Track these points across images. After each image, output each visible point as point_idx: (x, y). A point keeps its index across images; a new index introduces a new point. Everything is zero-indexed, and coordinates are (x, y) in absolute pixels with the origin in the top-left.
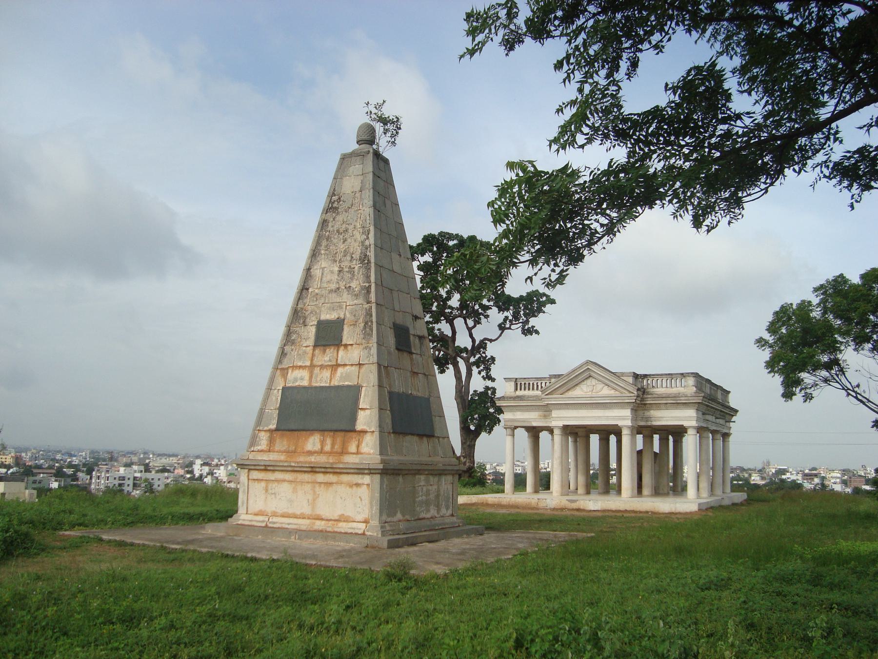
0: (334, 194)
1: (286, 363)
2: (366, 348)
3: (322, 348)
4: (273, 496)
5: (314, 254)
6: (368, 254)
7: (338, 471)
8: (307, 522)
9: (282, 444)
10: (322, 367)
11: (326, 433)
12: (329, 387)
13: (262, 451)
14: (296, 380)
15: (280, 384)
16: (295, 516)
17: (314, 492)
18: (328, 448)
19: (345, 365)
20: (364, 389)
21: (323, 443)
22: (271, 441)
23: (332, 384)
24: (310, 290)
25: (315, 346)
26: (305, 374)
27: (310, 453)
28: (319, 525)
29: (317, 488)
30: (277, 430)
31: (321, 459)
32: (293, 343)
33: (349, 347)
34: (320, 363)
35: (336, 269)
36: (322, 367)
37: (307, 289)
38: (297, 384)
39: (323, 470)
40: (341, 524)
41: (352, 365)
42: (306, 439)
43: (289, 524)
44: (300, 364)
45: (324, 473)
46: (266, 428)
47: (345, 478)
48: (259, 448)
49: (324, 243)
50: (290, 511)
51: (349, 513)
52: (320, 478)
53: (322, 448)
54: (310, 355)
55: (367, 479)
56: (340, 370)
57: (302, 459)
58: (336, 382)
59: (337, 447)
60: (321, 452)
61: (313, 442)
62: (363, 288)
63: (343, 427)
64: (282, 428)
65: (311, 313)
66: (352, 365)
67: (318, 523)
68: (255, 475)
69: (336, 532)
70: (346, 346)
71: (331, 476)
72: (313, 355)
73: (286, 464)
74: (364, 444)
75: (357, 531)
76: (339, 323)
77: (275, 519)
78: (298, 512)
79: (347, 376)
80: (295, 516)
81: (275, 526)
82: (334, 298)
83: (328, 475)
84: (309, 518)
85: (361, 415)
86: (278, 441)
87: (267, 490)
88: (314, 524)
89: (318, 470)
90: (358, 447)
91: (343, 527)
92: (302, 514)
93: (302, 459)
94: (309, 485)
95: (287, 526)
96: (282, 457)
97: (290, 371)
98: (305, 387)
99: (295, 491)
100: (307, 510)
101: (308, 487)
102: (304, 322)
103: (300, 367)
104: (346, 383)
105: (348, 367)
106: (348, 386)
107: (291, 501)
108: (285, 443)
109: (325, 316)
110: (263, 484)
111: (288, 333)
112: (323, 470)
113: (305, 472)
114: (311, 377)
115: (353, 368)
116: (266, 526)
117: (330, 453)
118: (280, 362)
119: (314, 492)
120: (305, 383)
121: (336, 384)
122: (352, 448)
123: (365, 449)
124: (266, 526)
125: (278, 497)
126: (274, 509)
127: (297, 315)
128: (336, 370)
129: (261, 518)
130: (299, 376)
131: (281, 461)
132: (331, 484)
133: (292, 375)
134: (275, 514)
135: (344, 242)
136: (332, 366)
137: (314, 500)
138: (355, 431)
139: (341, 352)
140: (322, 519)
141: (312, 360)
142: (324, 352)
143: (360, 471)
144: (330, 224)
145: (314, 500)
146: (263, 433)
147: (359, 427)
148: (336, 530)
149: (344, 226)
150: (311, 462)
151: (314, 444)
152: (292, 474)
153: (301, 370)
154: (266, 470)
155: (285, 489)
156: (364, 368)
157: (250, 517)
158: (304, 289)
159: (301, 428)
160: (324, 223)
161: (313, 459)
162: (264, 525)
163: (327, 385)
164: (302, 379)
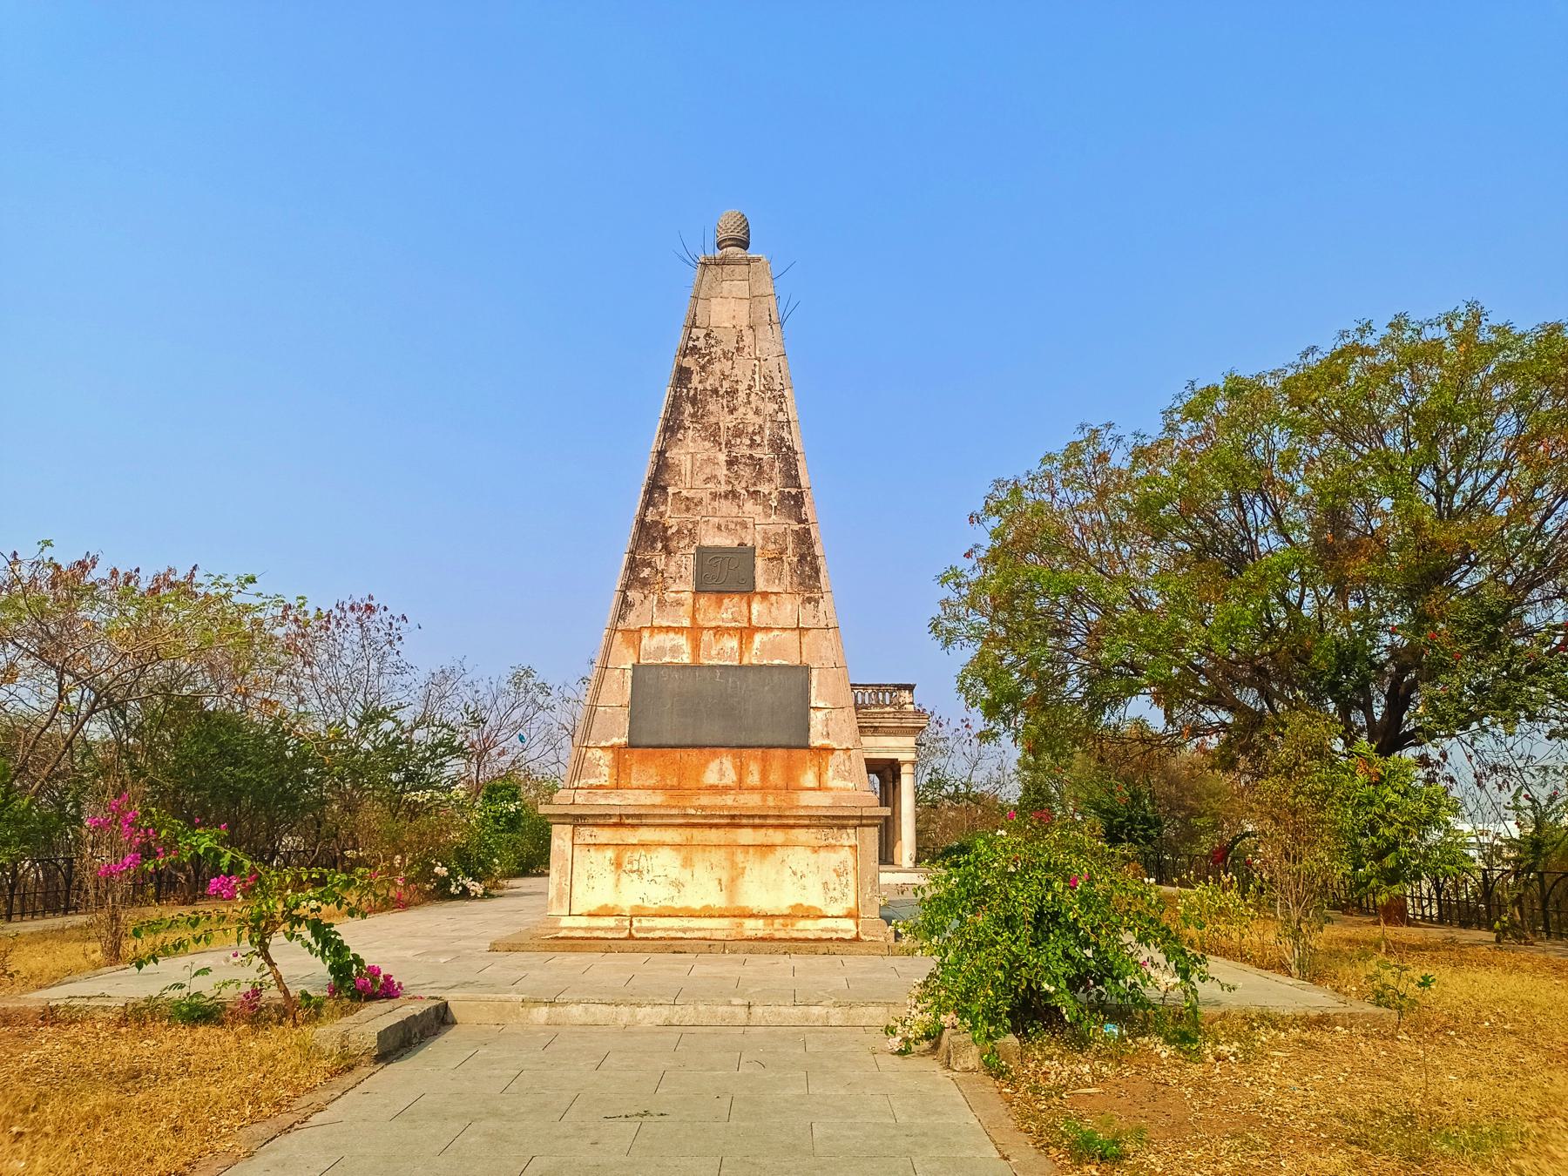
0: (694, 325)
1: (632, 620)
2: (809, 600)
3: (713, 597)
4: (635, 876)
5: (671, 428)
6: (785, 435)
7: (791, 822)
8: (725, 922)
9: (645, 773)
10: (718, 631)
11: (745, 752)
12: (741, 667)
13: (600, 787)
14: (661, 650)
15: (625, 659)
16: (692, 915)
17: (733, 864)
18: (754, 779)
19: (768, 629)
20: (814, 672)
21: (741, 771)
22: (620, 766)
23: (745, 661)
24: (671, 490)
25: (698, 592)
26: (682, 641)
27: (713, 788)
28: (753, 927)
29: (740, 857)
30: (631, 745)
31: (751, 801)
32: (645, 583)
33: (773, 598)
34: (713, 624)
35: (722, 457)
36: (718, 631)
37: (664, 489)
38: (667, 659)
39: (757, 821)
40: (801, 924)
41: (784, 629)
42: (705, 765)
43: (684, 930)
44: (665, 624)
45: (754, 826)
46: (603, 744)
47: (801, 835)
48: (592, 781)
49: (689, 409)
50: (678, 903)
51: (814, 899)
52: (746, 836)
53: (740, 780)
54: (688, 607)
55: (849, 837)
56: (758, 638)
57: (705, 800)
58: (751, 658)
59: (775, 777)
60: (740, 786)
61: (721, 770)
62: (783, 497)
63: (784, 741)
64: (644, 741)
65: (679, 531)
66: (784, 629)
67: (750, 924)
68: (585, 833)
69: (796, 940)
70: (765, 595)
71: (771, 831)
72: (695, 610)
73: (674, 812)
74: (830, 773)
75: (841, 935)
76: (745, 554)
77: (646, 923)
78: (697, 904)
79: (776, 649)
80: (692, 915)
81: (650, 935)
82: (726, 507)
83: (763, 831)
84: (721, 916)
85: (816, 718)
86: (634, 769)
87: (618, 865)
88: (741, 925)
89: (744, 821)
90: (820, 777)
91: (810, 928)
92: (707, 907)
93: (705, 800)
94: (722, 852)
95: (680, 935)
96: (658, 798)
97: (646, 634)
98: (685, 667)
99: (687, 863)
100: (718, 900)
101: (718, 856)
102: (665, 547)
103: (668, 629)
104: (776, 662)
105: (776, 633)
106: (779, 666)
107: (678, 885)
108: (652, 771)
109: (712, 539)
110: (610, 853)
111: (633, 566)
112: (757, 821)
113: (717, 826)
114: (696, 648)
115: (785, 634)
116: (631, 937)
117: (763, 788)
118: (621, 617)
119: (733, 864)
120: (686, 659)
121: (755, 662)
122: (809, 779)
123: (831, 780)
124: (631, 937)
125: (646, 877)
126: (639, 902)
127: (649, 534)
128: (751, 637)
129: (610, 922)
130: (668, 645)
131: (660, 806)
132: (772, 847)
133: (649, 642)
134: (639, 913)
135: (731, 412)
136: (741, 630)
137: (733, 880)
138: (808, 747)
139: (756, 607)
140: (752, 916)
141: (694, 618)
142: (720, 603)
143: (837, 822)
144: (695, 378)
145: (733, 880)
146: (599, 753)
147: (816, 740)
148: (795, 935)
149: (726, 384)
150: (730, 808)
151: (722, 774)
152: (680, 830)
153: (672, 635)
154: (620, 825)
155: (665, 862)
156: (808, 638)
157: (584, 922)
158: (656, 488)
159: (689, 741)
160: (683, 375)
161: (729, 800)
162: (625, 934)
163: (736, 663)
164: (675, 650)
